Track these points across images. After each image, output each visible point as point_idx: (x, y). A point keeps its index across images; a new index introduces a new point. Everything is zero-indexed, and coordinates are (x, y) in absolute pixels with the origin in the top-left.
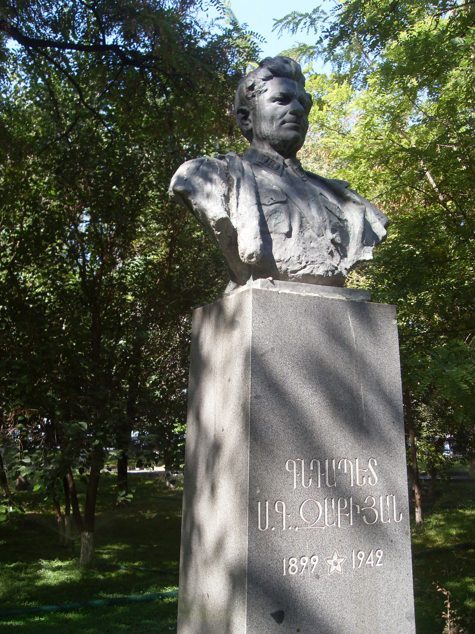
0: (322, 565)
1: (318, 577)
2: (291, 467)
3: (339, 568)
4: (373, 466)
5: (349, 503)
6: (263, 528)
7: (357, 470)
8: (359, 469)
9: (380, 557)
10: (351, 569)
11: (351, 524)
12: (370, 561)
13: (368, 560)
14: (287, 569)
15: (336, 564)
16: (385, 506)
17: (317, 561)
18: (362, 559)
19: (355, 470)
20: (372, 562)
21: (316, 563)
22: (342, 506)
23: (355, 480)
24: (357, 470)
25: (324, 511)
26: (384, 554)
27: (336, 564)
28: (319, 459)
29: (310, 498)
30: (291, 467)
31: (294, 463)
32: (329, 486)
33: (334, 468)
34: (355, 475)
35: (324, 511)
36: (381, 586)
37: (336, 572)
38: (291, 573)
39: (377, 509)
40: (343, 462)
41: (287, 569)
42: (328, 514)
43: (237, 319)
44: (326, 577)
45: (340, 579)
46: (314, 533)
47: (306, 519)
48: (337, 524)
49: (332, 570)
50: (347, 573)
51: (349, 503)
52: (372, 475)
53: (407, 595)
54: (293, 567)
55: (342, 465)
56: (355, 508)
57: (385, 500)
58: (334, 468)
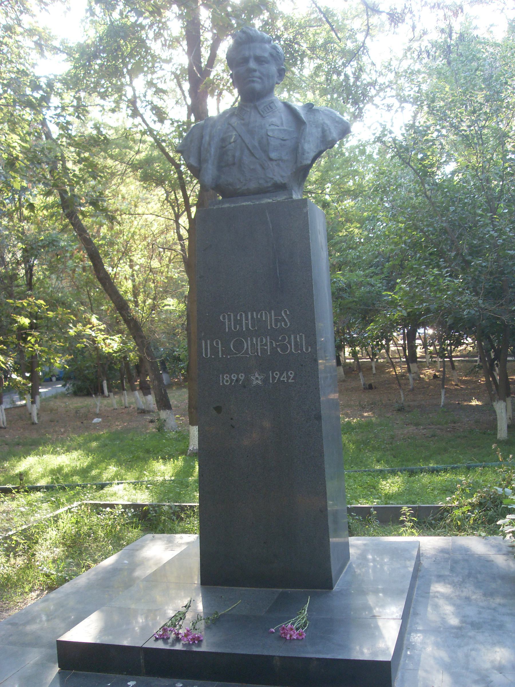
0: (248, 380)
1: (245, 387)
2: (224, 319)
3: (259, 382)
5: (267, 341)
6: (206, 355)
7: (273, 318)
9: (292, 376)
10: (269, 383)
14: (223, 381)
15: (257, 379)
16: (296, 342)
17: (244, 376)
18: (277, 377)
19: (271, 318)
20: (285, 379)
21: (242, 378)
22: (262, 341)
23: (271, 325)
24: (273, 318)
25: (248, 345)
26: (295, 373)
27: (257, 379)
28: (244, 312)
30: (224, 319)
34: (271, 321)
35: (248, 345)
37: (257, 385)
41: (223, 381)
48: (258, 353)
52: (284, 321)
56: (271, 343)
57: (295, 338)
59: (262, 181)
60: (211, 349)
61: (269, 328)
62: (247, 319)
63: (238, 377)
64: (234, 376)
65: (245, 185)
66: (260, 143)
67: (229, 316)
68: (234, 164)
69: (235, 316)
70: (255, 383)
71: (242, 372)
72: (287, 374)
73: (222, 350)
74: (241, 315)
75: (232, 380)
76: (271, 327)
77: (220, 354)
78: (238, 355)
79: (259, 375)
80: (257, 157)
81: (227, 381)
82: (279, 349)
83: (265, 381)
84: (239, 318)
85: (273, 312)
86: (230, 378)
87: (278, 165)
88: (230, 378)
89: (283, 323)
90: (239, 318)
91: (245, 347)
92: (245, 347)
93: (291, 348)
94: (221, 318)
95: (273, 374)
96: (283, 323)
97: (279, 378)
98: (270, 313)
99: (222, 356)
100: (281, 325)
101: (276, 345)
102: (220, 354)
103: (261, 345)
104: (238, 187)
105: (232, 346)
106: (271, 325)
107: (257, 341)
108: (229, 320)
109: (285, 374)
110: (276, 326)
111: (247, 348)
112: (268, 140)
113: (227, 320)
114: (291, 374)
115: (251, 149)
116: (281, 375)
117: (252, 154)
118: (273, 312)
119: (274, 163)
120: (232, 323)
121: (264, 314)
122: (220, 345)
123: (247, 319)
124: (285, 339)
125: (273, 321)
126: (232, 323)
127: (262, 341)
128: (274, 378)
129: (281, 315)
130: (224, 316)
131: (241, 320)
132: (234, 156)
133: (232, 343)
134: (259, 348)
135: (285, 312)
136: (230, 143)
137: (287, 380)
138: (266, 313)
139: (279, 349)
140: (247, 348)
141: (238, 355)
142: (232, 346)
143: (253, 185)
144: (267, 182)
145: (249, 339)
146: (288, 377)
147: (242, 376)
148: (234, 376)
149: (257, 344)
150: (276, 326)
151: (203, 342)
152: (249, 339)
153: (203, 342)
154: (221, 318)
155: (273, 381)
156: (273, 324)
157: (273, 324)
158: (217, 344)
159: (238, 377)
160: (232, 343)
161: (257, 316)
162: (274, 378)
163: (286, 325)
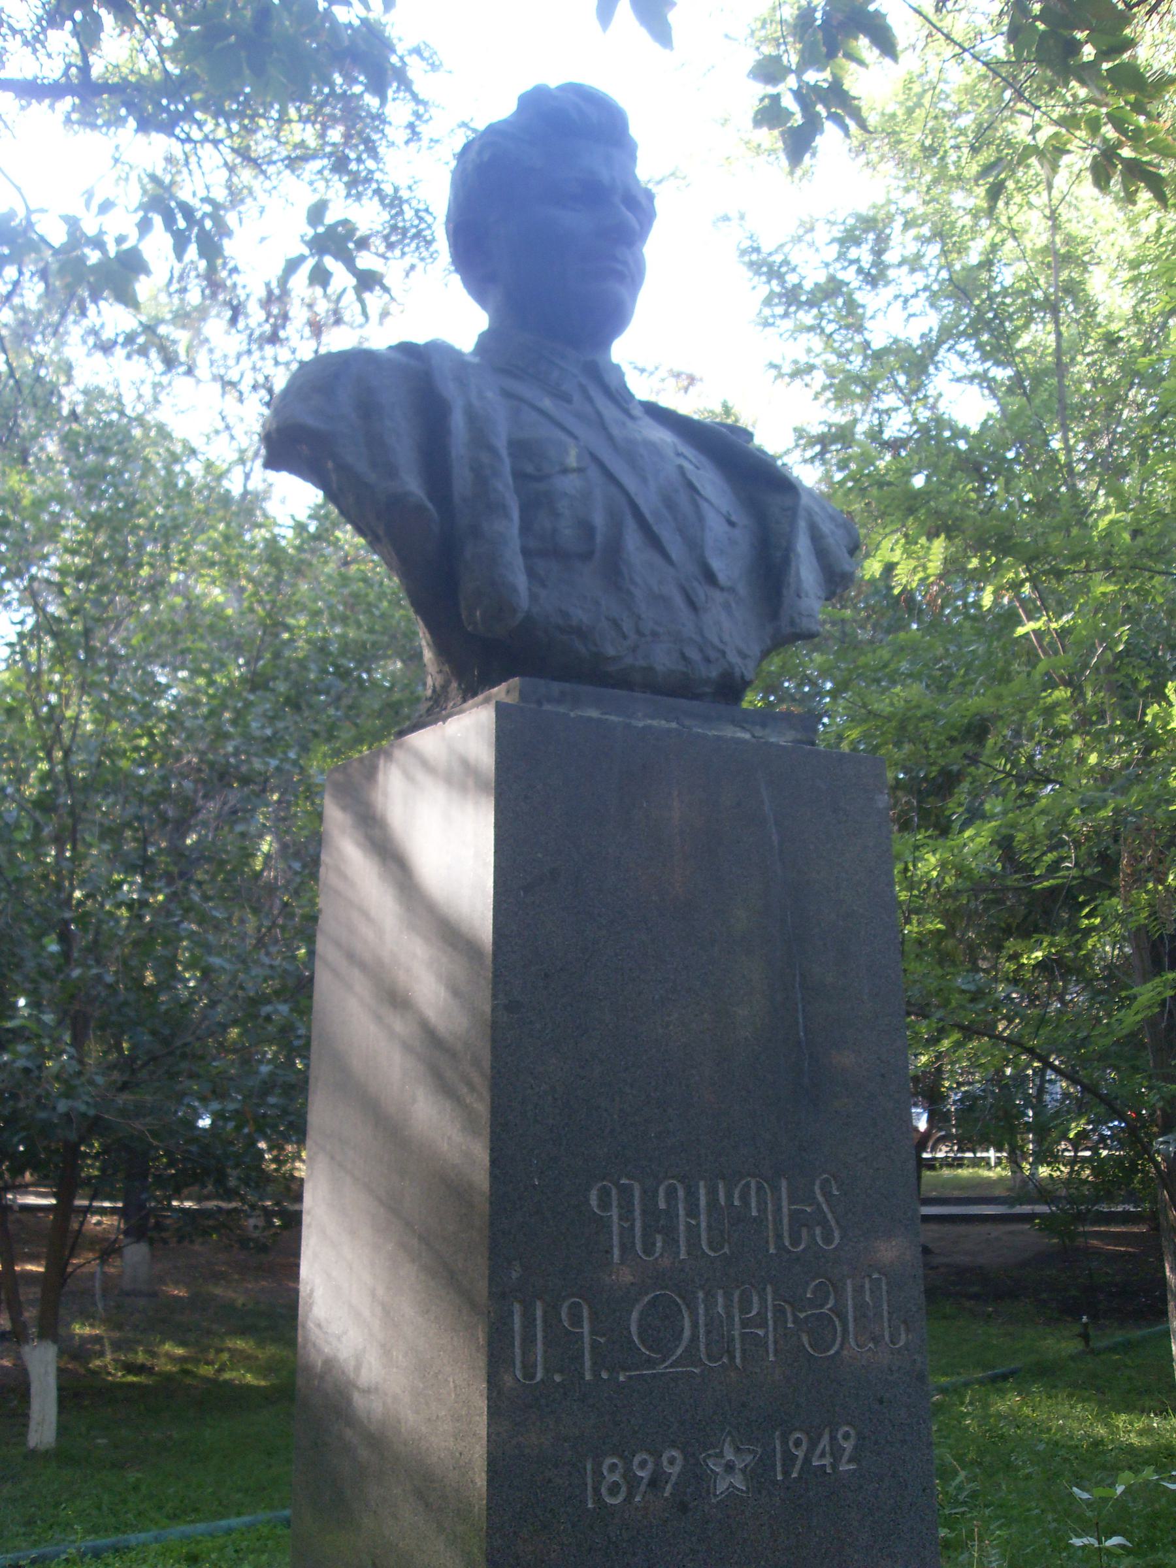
0: (697, 1476)
1: (683, 1508)
2: (605, 1204)
3: (738, 1482)
4: (827, 1195)
5: (763, 1300)
8: (791, 1203)
9: (848, 1445)
10: (774, 1482)
11: (771, 1358)
12: (823, 1455)
13: (818, 1452)
14: (597, 1491)
15: (730, 1468)
18: (800, 1453)
19: (779, 1209)
20: (827, 1461)
21: (674, 1470)
23: (779, 1236)
25: (695, 1325)
26: (861, 1437)
27: (730, 1468)
29: (662, 1288)
30: (605, 1204)
31: (614, 1192)
32: (712, 1254)
33: (722, 1201)
34: (778, 1222)
36: (856, 1524)
38: (610, 1500)
39: (838, 1316)
40: (748, 1185)
41: (597, 1491)
42: (708, 1332)
43: (961, 426)
44: (707, 1508)
45: (743, 1512)
46: (672, 1385)
47: (650, 1348)
48: (732, 1358)
49: (722, 1487)
50: (764, 1493)
51: (763, 1300)
52: (824, 1223)
53: (924, 1547)
54: (616, 1484)
55: (745, 1197)
56: (779, 1312)
57: (859, 1290)
58: (722, 1201)
59: (694, 654)
60: (547, 1343)
61: (772, 1251)
62: (692, 1211)
63: (658, 1464)
64: (642, 1466)
65: (634, 649)
66: (670, 504)
67: (625, 1191)
68: (587, 556)
69: (649, 1195)
70: (722, 1487)
71: (673, 1445)
72: (833, 1438)
73: (595, 1346)
74: (671, 1193)
75: (632, 1482)
76: (780, 1247)
77: (588, 1364)
78: (660, 1369)
79: (738, 1450)
80: (674, 556)
81: (614, 1489)
82: (805, 1339)
83: (759, 1475)
84: (662, 1205)
85: (784, 1184)
86: (628, 1475)
87: (727, 607)
88: (628, 1475)
89: (818, 1231)
90: (662, 1205)
91: (687, 1333)
92: (687, 1333)
93: (845, 1330)
94: (594, 1202)
95: (785, 1443)
96: (818, 1231)
97: (807, 1460)
98: (775, 1189)
99: (596, 1374)
100: (813, 1237)
101: (796, 1320)
102: (588, 1364)
103: (745, 1324)
104: (611, 651)
105: (634, 1329)
106: (779, 1236)
107: (728, 1307)
108: (627, 1213)
109: (825, 1441)
110: (795, 1242)
111: (694, 1338)
112: (697, 507)
113: (615, 1213)
114: (846, 1436)
115: (648, 516)
116: (813, 1444)
117: (654, 541)
118: (784, 1184)
119: (718, 596)
120: (638, 1225)
121: (753, 1192)
122: (586, 1329)
123: (692, 1211)
124: (827, 1299)
125: (786, 1221)
126: (638, 1225)
127: (745, 1306)
128: (789, 1459)
129: (812, 1200)
130: (605, 1194)
131: (671, 1214)
132: (588, 529)
133: (635, 1315)
134: (736, 1333)
135: (825, 1184)
136: (565, 471)
137: (834, 1466)
138: (760, 1188)
139: (805, 1339)
140: (694, 1338)
141: (660, 1369)
142: (634, 1329)
143: (663, 659)
144: (708, 660)
145: (701, 1295)
146: (836, 1453)
147: (672, 1461)
148: (642, 1466)
149: (730, 1316)
150: (795, 1242)
151: (517, 1307)
152: (701, 1295)
153: (517, 1307)
154: (594, 1202)
155: (786, 1473)
156: (786, 1234)
157: (786, 1234)
158: (576, 1320)
159: (658, 1464)
160: (635, 1315)
161: (729, 1196)
162: (789, 1459)
163: (828, 1239)
